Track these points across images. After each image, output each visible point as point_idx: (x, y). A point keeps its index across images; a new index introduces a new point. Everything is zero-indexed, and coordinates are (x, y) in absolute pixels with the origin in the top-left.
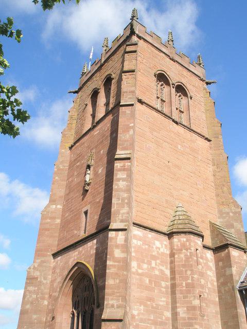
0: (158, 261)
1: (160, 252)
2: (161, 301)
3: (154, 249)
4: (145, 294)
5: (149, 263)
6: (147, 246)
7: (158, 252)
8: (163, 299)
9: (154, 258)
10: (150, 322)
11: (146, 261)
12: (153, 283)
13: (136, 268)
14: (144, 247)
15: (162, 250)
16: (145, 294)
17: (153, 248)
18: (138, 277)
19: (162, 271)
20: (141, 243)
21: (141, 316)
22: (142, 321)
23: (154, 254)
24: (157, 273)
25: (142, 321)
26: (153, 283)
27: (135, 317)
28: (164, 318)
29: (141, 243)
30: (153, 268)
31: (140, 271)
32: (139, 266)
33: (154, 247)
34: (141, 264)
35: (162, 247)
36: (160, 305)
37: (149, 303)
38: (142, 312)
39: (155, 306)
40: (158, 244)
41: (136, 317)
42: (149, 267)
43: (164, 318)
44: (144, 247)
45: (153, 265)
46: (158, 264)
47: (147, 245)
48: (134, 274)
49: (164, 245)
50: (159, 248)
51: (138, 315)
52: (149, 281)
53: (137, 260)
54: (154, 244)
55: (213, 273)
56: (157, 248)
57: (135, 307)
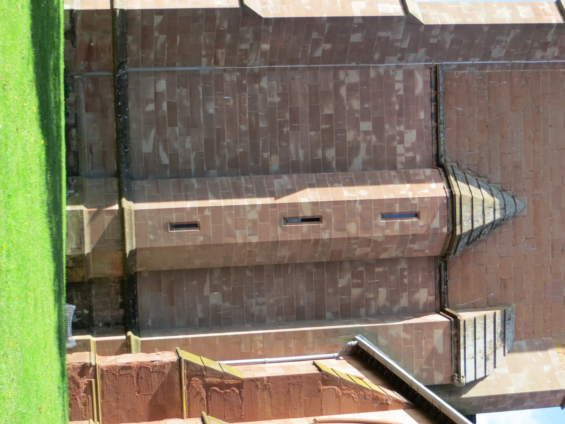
0: (374, 138)
1: (395, 143)
2: (296, 148)
3: (398, 128)
4: (302, 104)
5: (365, 115)
6: (397, 107)
7: (392, 138)
8: (301, 152)
9: (378, 129)
10: (254, 119)
11: (366, 106)
12: (328, 126)
13: (347, 81)
14: (394, 99)
15: (400, 149)
16: (302, 104)
17: (399, 123)
18: (331, 86)
19: (355, 149)
20: (401, 92)
21: (260, 96)
22: (253, 98)
23: (387, 126)
24: (350, 136)
25: (253, 98)
26: (328, 126)
27: (256, 83)
28: (266, 155)
29: (401, 92)
30: (356, 126)
31: (343, 91)
32: (352, 88)
33: (402, 128)
34: (358, 94)
35: (407, 150)
36: (288, 142)
37: (287, 115)
38: (269, 100)
39: (285, 130)
40: (411, 136)
41: (257, 86)
42: (357, 115)
43: (266, 155)
44: (394, 99)
45: (366, 126)
46: (368, 138)
47: (401, 108)
48: (336, 76)
49: (411, 154)
50: (401, 142)
51: (261, 89)
52: (330, 116)
53: (365, 82)
54: (408, 128)
55: (384, 306)
56: (401, 134)
57: (274, 83)
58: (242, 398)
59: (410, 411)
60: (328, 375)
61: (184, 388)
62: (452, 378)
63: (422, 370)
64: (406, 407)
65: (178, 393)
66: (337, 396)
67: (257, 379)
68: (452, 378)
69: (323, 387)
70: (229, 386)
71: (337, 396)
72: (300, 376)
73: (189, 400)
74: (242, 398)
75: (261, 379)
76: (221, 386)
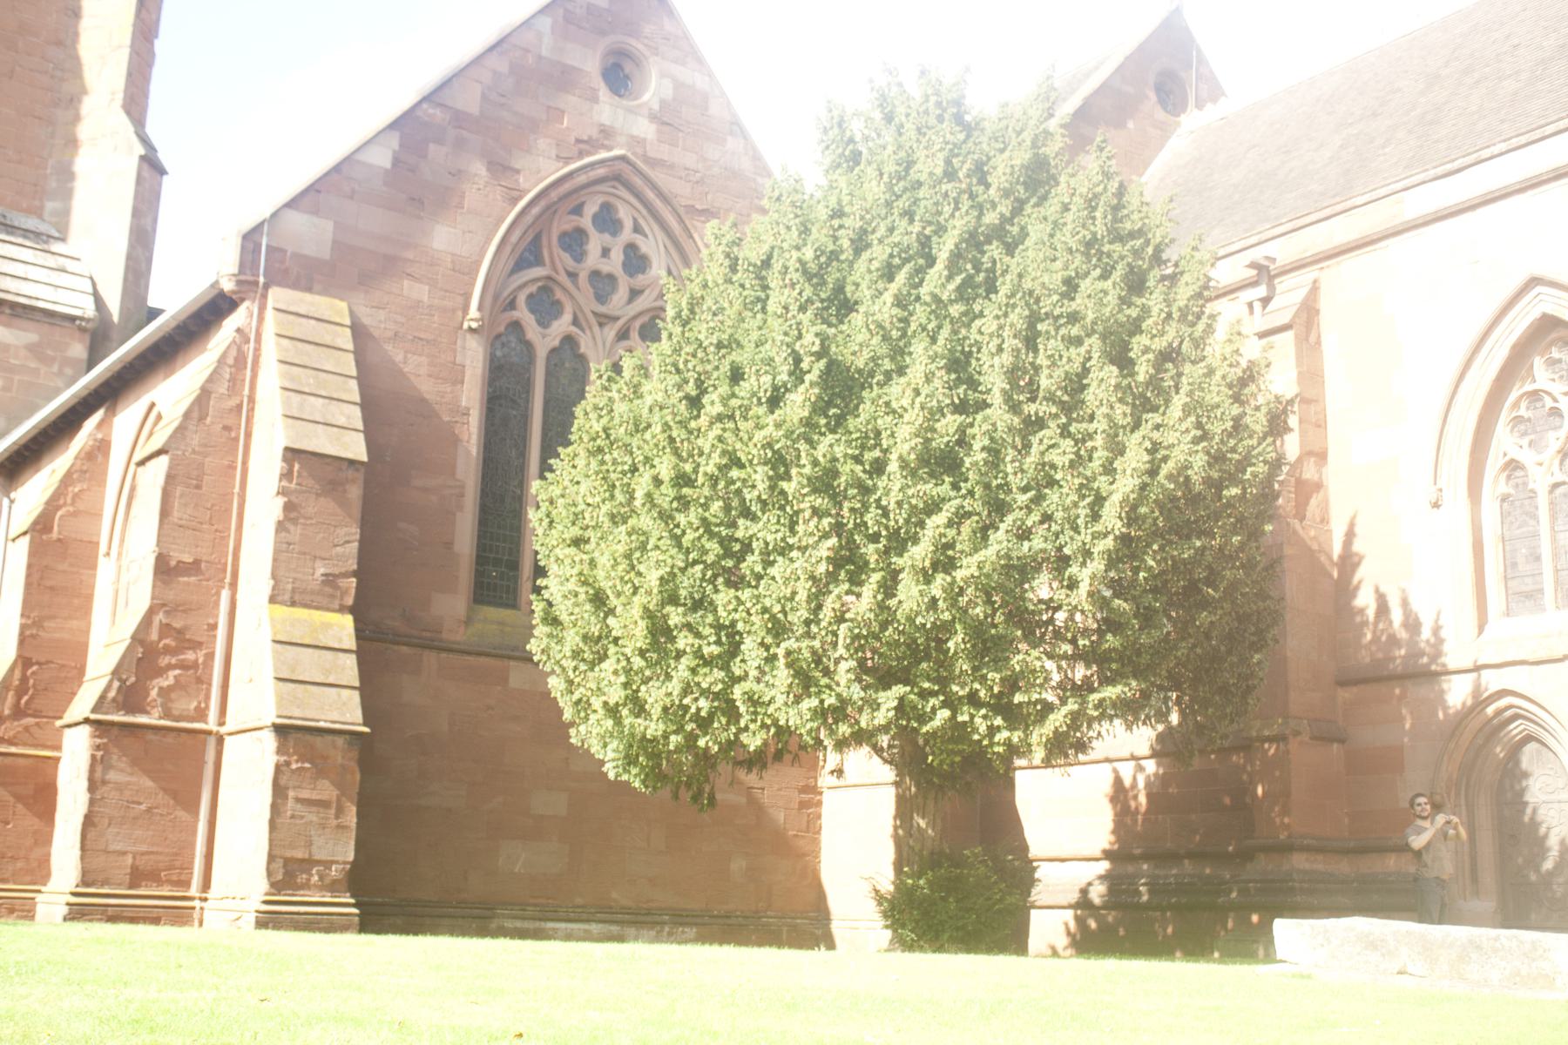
58: (48, 662)
59: (120, 406)
60: (36, 523)
61: (13, 750)
62: (82, 330)
63: (60, 373)
64: (112, 412)
65: (21, 761)
66: (75, 514)
67: (22, 634)
68: (82, 330)
69: (55, 535)
70: (24, 679)
71: (75, 514)
72: (29, 566)
73: (36, 746)
74: (48, 662)
75: (23, 628)
76: (21, 691)
